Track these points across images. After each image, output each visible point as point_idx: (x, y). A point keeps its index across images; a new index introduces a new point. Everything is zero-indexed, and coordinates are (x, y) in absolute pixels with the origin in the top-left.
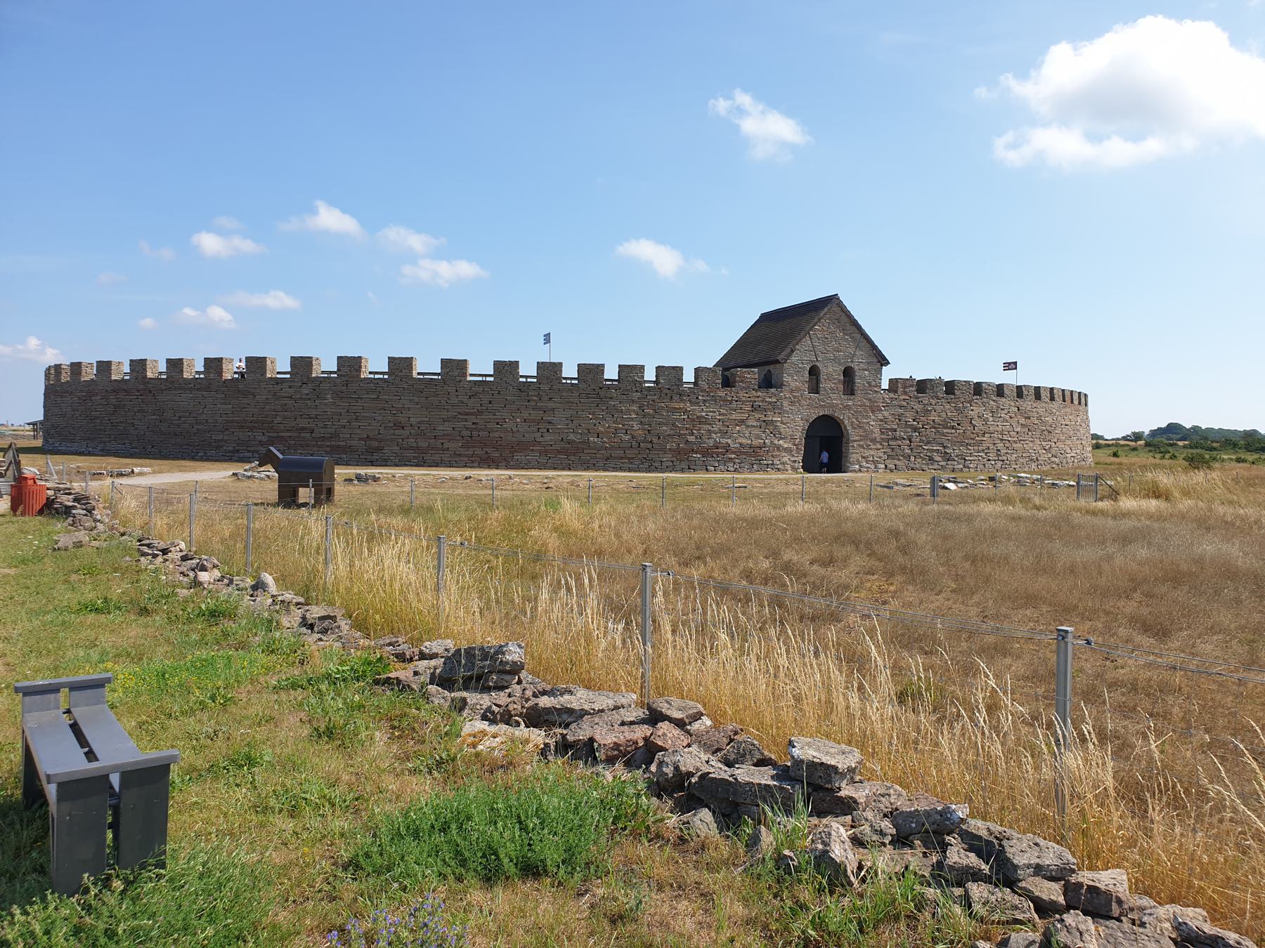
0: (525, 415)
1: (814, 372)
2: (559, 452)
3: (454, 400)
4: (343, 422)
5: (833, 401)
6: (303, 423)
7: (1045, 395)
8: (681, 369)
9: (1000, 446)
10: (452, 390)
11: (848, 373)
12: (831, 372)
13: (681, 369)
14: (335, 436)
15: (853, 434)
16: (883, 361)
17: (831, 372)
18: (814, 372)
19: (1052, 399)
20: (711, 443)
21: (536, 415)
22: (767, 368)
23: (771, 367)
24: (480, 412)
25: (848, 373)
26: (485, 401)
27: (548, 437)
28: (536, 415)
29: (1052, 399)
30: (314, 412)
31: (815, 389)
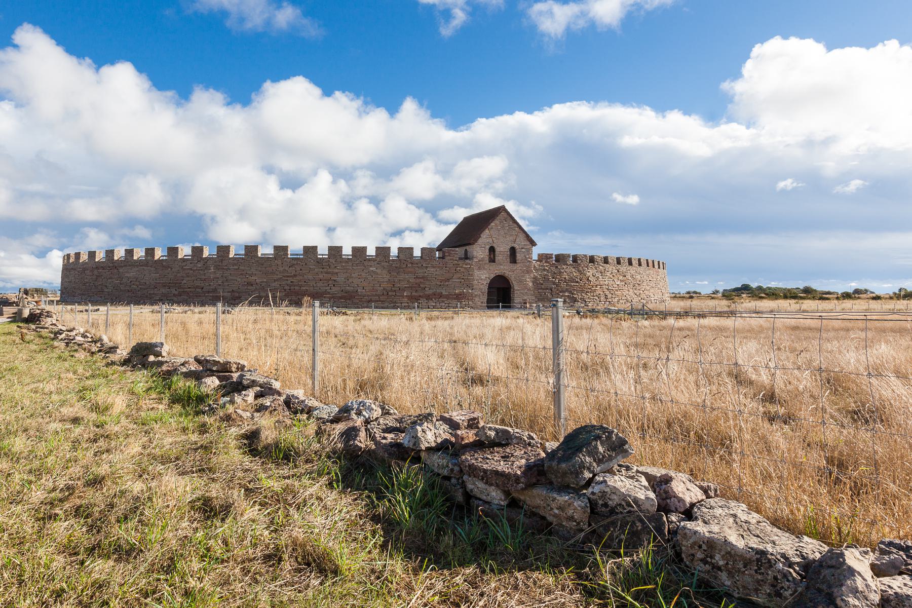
0: (321, 276)
1: (492, 250)
2: (341, 298)
3: (281, 269)
4: (220, 282)
5: (503, 268)
6: (198, 283)
7: (635, 262)
8: (412, 249)
9: (607, 293)
10: (279, 263)
11: (513, 251)
12: (502, 249)
13: (412, 249)
14: (215, 290)
15: (516, 286)
16: (533, 243)
17: (502, 249)
18: (492, 250)
19: (640, 265)
20: (431, 292)
21: (328, 276)
22: (465, 248)
23: (467, 248)
24: (295, 276)
25: (513, 251)
26: (298, 269)
27: (334, 289)
28: (328, 276)
29: (640, 265)
30: (203, 277)
31: (492, 260)
